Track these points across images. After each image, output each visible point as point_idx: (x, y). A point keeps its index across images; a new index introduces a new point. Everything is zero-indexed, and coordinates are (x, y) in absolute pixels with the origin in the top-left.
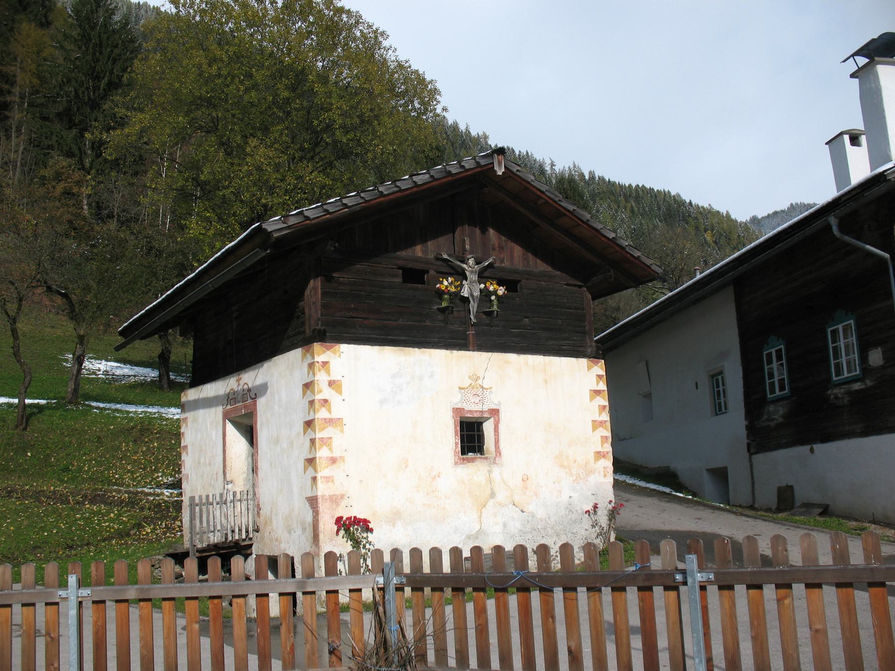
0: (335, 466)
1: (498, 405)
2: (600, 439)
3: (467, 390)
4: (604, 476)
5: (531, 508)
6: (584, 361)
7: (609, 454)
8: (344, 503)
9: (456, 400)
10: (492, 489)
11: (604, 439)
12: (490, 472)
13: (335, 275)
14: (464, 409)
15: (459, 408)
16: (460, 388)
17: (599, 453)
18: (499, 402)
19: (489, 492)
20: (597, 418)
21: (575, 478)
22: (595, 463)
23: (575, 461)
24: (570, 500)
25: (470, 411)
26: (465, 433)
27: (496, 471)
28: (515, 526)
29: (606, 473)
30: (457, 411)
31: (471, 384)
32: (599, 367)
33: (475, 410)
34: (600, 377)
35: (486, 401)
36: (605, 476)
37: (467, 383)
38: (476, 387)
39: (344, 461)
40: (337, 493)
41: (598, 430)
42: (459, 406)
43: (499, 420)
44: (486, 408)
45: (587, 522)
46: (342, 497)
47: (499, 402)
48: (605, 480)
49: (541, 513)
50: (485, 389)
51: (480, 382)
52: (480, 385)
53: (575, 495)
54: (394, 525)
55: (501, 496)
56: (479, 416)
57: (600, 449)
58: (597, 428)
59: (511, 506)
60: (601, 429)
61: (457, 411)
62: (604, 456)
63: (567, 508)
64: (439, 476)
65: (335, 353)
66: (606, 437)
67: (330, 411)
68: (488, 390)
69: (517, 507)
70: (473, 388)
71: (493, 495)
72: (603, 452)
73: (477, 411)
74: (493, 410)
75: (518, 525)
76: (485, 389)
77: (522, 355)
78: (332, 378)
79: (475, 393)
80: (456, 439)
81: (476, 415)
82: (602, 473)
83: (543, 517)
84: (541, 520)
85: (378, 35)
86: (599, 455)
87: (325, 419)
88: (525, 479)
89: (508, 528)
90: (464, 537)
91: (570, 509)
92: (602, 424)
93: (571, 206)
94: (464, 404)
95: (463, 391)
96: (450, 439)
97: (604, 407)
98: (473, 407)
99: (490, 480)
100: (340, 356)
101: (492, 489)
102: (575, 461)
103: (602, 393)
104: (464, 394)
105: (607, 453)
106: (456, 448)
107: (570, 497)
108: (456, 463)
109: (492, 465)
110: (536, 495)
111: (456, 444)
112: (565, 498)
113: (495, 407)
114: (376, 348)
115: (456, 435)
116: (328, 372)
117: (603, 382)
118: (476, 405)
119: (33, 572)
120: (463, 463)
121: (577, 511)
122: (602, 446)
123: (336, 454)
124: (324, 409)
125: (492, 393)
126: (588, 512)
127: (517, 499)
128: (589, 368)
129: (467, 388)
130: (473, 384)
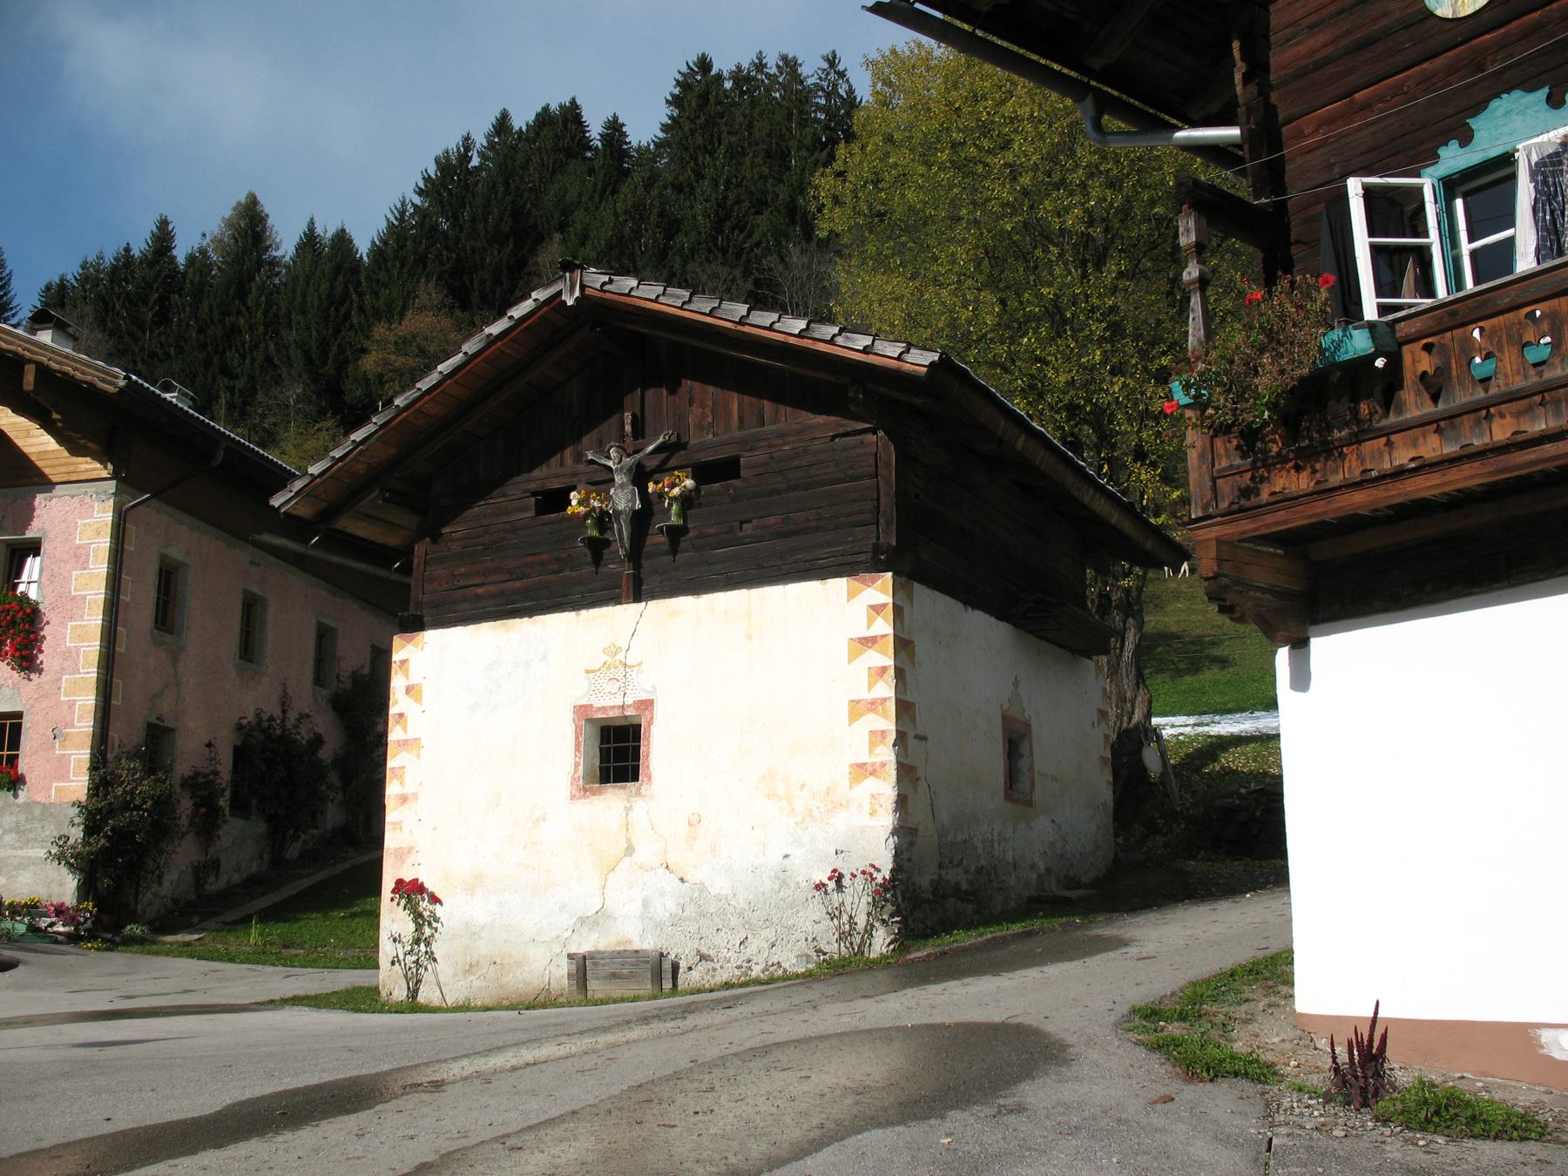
0: (406, 806)
1: (650, 692)
2: (866, 737)
3: (598, 674)
4: (871, 814)
5: (694, 876)
6: (839, 585)
7: (887, 768)
8: (411, 859)
9: (582, 692)
10: (628, 840)
11: (877, 736)
12: (628, 810)
13: (446, 530)
14: (592, 705)
15: (584, 706)
16: (588, 672)
17: (862, 766)
18: (653, 686)
19: (623, 845)
20: (864, 694)
21: (799, 819)
22: (851, 788)
23: (803, 786)
24: (786, 861)
25: (603, 709)
26: (612, 745)
27: (639, 806)
28: (665, 907)
29: (877, 807)
30: (581, 710)
31: (605, 663)
32: (876, 589)
33: (612, 704)
34: (877, 609)
35: (630, 687)
36: (873, 813)
37: (598, 660)
38: (618, 665)
39: (416, 800)
40: (404, 845)
41: (864, 718)
42: (585, 702)
43: (652, 718)
44: (629, 700)
45: (816, 910)
46: (410, 850)
47: (653, 686)
48: (874, 822)
49: (720, 885)
50: (629, 667)
51: (621, 656)
52: (621, 662)
53: (798, 854)
54: (472, 894)
55: (644, 853)
56: (617, 715)
57: (864, 758)
58: (861, 715)
59: (662, 870)
60: (871, 716)
61: (581, 710)
62: (873, 773)
63: (777, 877)
64: (544, 819)
65: (417, 646)
66: (883, 732)
67: (405, 729)
68: (635, 669)
69: (671, 872)
70: (608, 669)
71: (630, 850)
72: (873, 764)
73: (613, 707)
74: (642, 702)
75: (671, 906)
76: (629, 667)
77: (704, 596)
78: (412, 682)
79: (611, 676)
80: (576, 756)
81: (611, 714)
82: (867, 808)
83: (723, 893)
84: (718, 898)
85: (267, 215)
86: (862, 771)
87: (399, 741)
88: (694, 822)
89: (652, 910)
90: (574, 920)
91: (783, 877)
92: (874, 705)
93: (705, 305)
94: (593, 698)
95: (592, 675)
96: (658, 751)
97: (884, 670)
98: (611, 701)
99: (627, 825)
100: (422, 649)
101: (628, 840)
102: (803, 786)
103: (881, 642)
104: (593, 681)
105: (883, 765)
106: (575, 772)
107: (786, 856)
108: (573, 797)
109: (633, 799)
110: (714, 851)
111: (577, 765)
112: (774, 859)
113: (644, 696)
114: (471, 628)
115: (577, 749)
116: (407, 676)
117: (885, 619)
118: (612, 697)
119: (629, 948)
120: (584, 797)
121: (798, 883)
122: (871, 751)
123: (408, 790)
124: (398, 727)
125: (642, 673)
126: (820, 886)
127: (673, 859)
128: (851, 595)
129: (599, 669)
130: (610, 660)
